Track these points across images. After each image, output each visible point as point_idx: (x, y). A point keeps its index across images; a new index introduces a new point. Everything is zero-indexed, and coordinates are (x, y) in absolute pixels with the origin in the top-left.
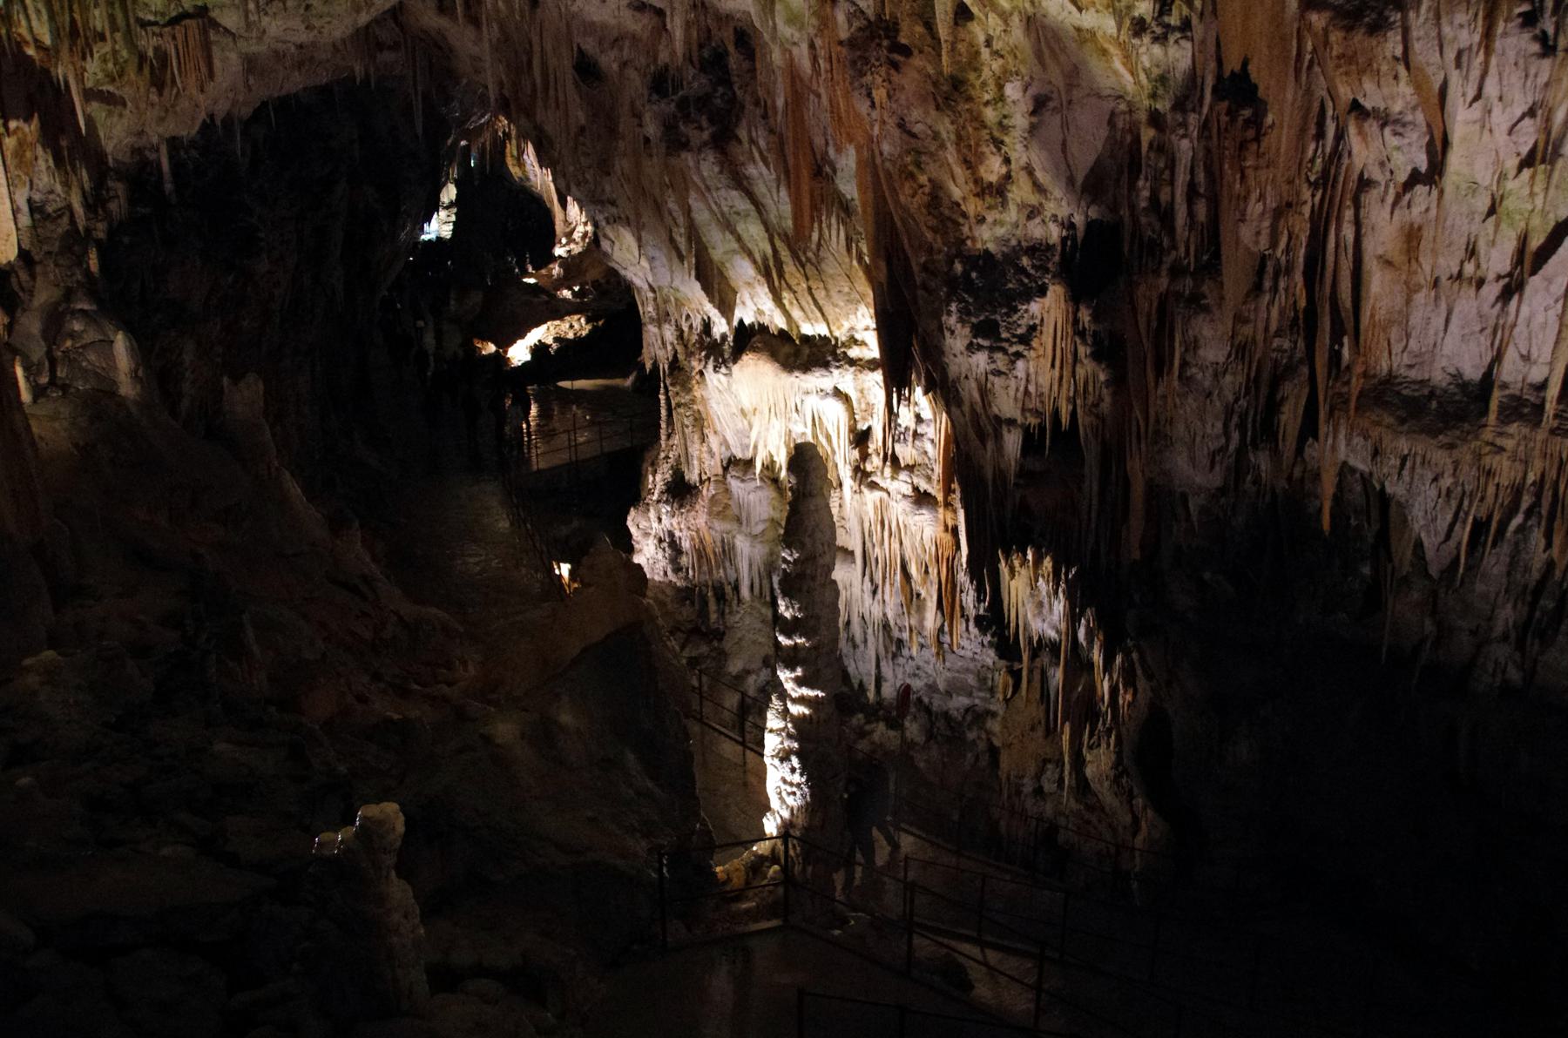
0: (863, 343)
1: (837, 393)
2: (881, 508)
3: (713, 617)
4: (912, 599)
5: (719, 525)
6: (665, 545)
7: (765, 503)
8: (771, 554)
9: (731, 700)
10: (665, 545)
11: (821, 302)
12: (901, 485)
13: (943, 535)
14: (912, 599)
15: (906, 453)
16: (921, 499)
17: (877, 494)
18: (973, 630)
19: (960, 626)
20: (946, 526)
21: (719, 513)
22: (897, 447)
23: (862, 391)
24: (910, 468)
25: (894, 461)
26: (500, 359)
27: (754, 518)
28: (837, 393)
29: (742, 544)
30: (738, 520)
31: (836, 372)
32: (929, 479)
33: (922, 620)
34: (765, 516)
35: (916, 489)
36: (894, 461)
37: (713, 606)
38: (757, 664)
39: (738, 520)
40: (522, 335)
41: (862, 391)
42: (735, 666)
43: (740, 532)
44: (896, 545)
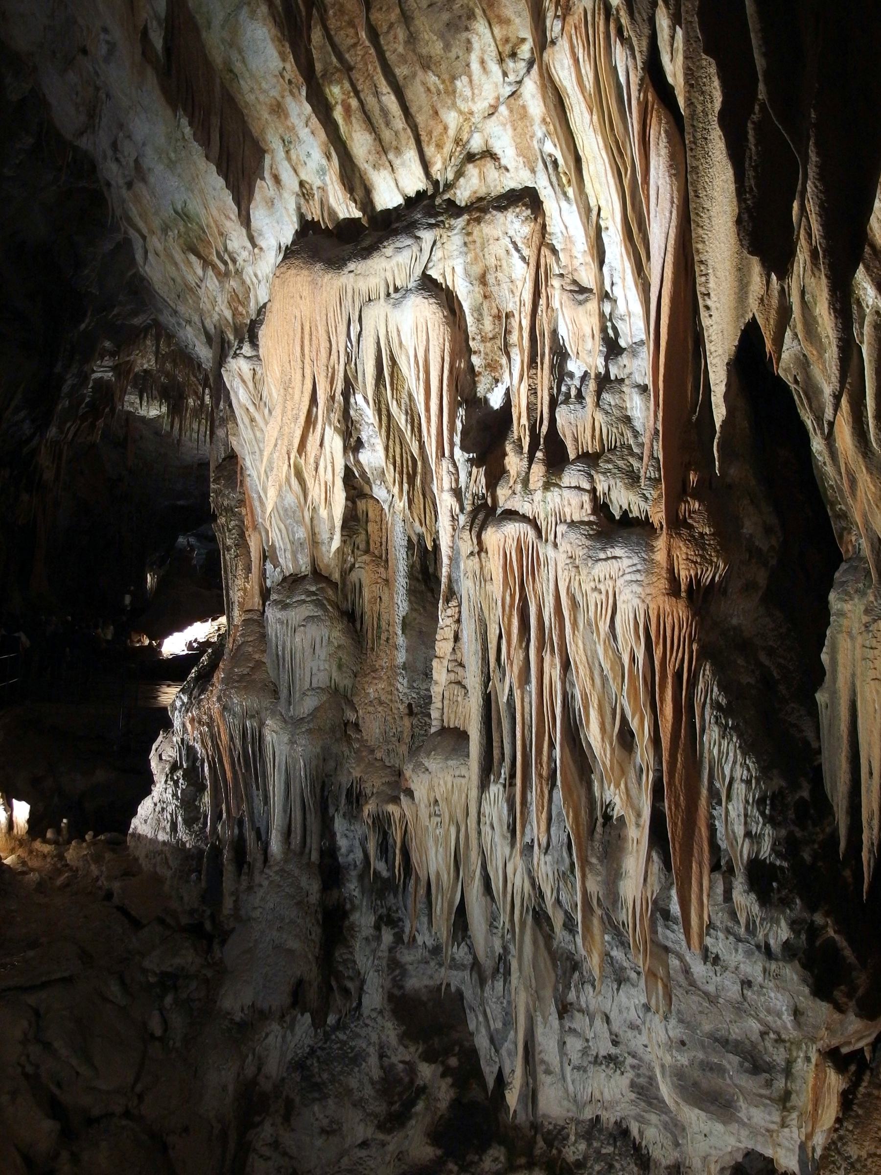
1: (429, 285)
2: (523, 569)
3: (228, 903)
4: (600, 832)
5: (238, 701)
6: (180, 773)
7: (322, 653)
8: (325, 756)
9: (221, 1078)
10: (180, 773)
11: (401, 71)
12: (567, 500)
13: (666, 604)
14: (600, 832)
15: (577, 424)
16: (609, 527)
17: (512, 529)
18: (744, 899)
19: (703, 879)
20: (673, 580)
21: (242, 677)
22: (563, 415)
23: (483, 280)
24: (590, 459)
25: (555, 456)
26: (155, 651)
27: (303, 681)
28: (429, 285)
29: (274, 736)
30: (275, 693)
31: (427, 236)
32: (632, 479)
33: (613, 876)
34: (321, 679)
35: (601, 507)
36: (555, 456)
37: (228, 883)
38: (279, 999)
40: (180, 628)
41: (483, 280)
42: (235, 1000)
43: (273, 713)
44: (553, 670)
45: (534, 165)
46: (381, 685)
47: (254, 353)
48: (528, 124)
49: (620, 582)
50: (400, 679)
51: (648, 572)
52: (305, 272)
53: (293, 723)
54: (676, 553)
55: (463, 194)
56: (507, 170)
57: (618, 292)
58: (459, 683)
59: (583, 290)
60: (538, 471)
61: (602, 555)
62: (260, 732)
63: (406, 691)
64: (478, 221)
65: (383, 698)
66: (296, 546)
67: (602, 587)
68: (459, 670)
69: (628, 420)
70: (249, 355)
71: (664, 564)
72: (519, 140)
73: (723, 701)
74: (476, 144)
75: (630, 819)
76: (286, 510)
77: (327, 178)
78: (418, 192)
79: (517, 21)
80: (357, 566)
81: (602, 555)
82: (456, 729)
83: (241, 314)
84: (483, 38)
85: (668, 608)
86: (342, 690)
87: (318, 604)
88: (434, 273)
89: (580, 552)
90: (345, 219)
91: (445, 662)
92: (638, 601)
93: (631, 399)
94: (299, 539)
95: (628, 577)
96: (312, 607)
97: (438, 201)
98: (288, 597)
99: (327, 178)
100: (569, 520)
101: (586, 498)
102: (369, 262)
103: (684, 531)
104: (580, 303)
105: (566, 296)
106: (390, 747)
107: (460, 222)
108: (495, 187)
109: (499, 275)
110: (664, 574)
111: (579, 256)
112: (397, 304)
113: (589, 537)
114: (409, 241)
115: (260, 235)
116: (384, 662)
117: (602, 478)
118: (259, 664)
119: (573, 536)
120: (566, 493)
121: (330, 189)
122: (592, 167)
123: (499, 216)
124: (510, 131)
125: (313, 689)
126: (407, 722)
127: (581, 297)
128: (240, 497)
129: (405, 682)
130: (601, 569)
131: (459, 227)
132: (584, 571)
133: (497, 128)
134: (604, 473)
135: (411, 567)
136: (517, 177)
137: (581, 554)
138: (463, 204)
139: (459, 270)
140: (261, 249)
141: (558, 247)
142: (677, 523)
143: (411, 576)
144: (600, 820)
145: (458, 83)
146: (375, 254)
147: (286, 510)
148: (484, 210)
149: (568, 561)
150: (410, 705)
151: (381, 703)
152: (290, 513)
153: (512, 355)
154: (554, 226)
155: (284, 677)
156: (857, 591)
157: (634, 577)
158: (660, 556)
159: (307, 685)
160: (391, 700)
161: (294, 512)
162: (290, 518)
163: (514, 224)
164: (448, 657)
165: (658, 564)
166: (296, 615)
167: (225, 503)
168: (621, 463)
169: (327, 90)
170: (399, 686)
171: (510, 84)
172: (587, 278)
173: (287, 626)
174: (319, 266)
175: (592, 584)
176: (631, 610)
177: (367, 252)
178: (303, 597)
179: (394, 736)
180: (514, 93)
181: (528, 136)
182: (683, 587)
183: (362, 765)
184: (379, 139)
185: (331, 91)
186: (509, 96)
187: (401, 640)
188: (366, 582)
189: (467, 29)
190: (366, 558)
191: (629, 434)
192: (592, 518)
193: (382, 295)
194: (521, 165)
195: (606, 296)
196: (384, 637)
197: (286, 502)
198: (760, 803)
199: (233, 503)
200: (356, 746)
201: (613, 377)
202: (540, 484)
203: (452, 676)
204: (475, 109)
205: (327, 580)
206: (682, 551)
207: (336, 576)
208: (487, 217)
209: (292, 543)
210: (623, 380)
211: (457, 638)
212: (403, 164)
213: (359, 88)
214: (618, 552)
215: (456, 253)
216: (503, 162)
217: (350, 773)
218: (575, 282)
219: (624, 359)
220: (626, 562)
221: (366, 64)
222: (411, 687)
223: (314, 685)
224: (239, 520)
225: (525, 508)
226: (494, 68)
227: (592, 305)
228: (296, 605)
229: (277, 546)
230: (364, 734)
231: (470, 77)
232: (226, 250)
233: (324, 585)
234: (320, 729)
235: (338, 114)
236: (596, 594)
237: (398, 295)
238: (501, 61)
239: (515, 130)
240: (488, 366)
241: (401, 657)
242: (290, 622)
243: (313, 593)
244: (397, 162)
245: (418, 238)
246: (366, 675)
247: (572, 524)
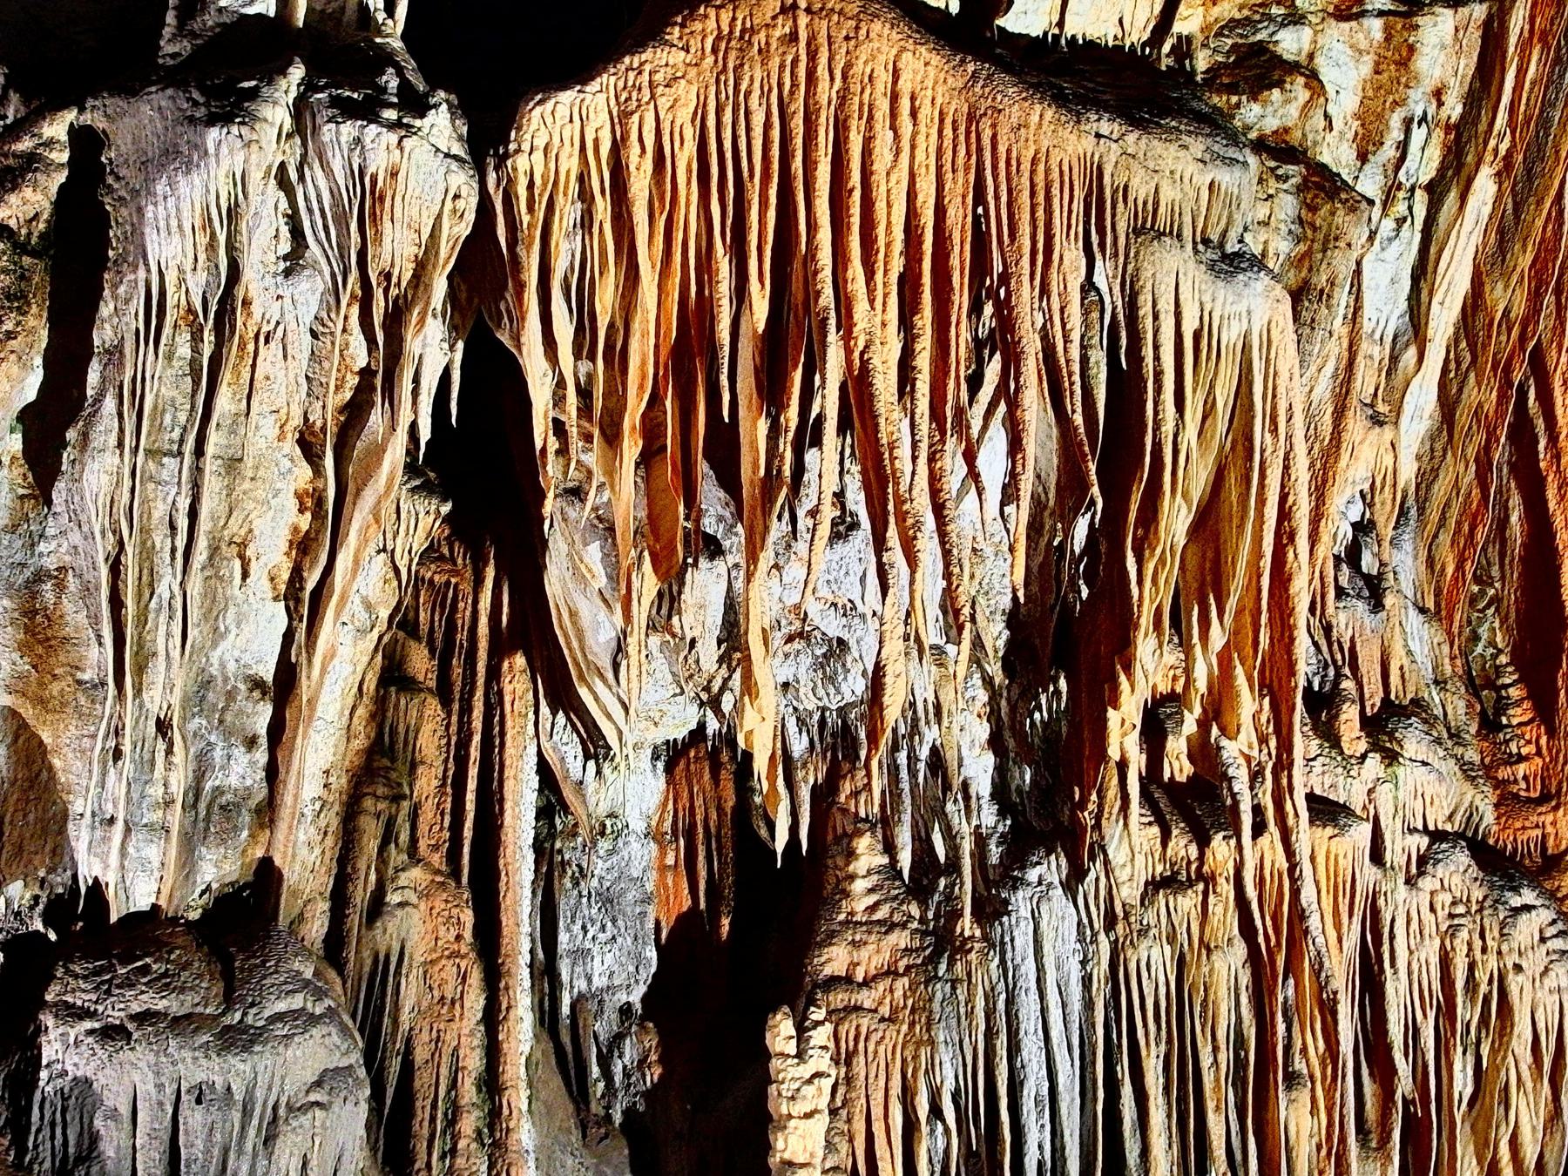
45: (1371, 148)
48: (1403, 80)
72: (1370, 93)
74: (1290, 43)
76: (206, 684)
80: (393, 898)
94: (218, 791)
98: (229, 1001)
100: (1431, 827)
124: (1366, 68)
131: (1293, 181)
133: (1340, 46)
164: (817, 1161)
173: (247, 1113)
178: (297, 1002)
181: (1391, 99)
188: (419, 951)
190: (416, 874)
194: (1350, 135)
196: (469, 1123)
202: (1362, 746)
228: (281, 1030)
229: (77, 806)
239: (1377, 72)
242: (259, 1094)
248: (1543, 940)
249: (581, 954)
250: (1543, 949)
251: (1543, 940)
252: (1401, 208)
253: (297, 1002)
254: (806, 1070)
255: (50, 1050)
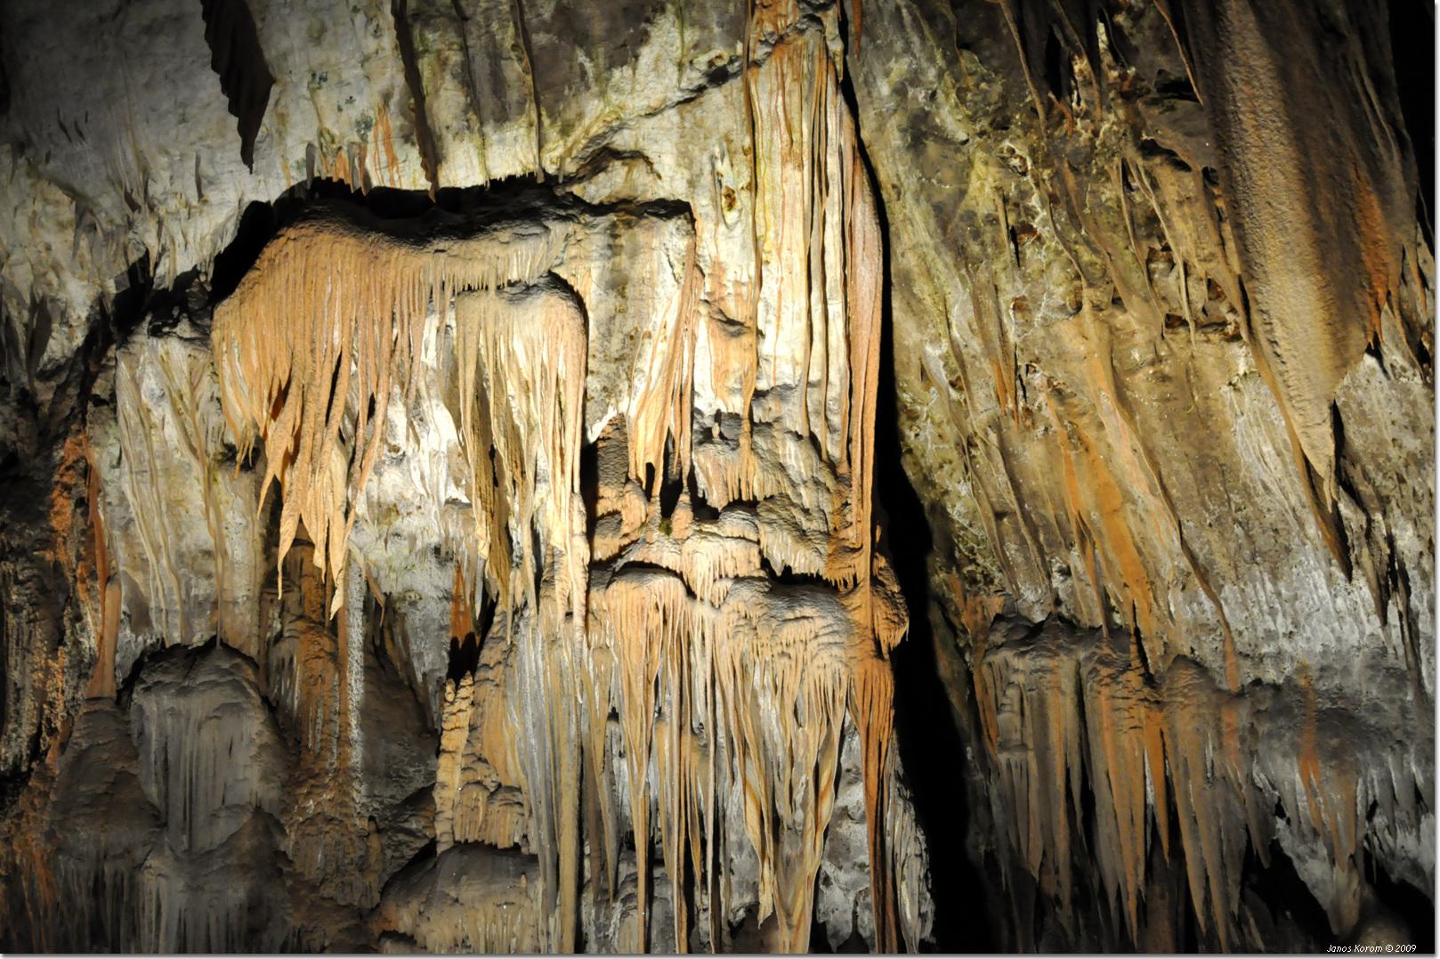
0: (636, 156)
17: (659, 583)
21: (95, 800)
28: (557, 283)
31: (558, 229)
32: (802, 535)
35: (765, 564)
39: (158, 819)
46: (327, 796)
47: (194, 335)
49: (812, 645)
50: (356, 785)
51: (849, 633)
52: (352, 241)
53: (196, 860)
54: (878, 613)
55: (596, 190)
56: (659, 177)
57: (769, 331)
58: (479, 783)
59: (731, 322)
60: (683, 515)
61: (790, 615)
62: (132, 878)
63: (364, 800)
64: (629, 225)
65: (329, 811)
66: (194, 607)
67: (792, 651)
68: (480, 766)
69: (782, 468)
70: (187, 335)
71: (866, 622)
73: (901, 772)
74: (622, 141)
75: (781, 920)
76: (181, 556)
77: (370, 135)
78: (511, 178)
79: (717, 30)
81: (790, 615)
82: (478, 845)
83: (49, 284)
84: (667, 37)
85: (876, 672)
86: (266, 809)
87: (238, 687)
88: (563, 273)
89: (755, 613)
90: (379, 188)
91: (459, 758)
92: (839, 666)
93: (784, 446)
95: (825, 639)
96: (228, 691)
97: (559, 192)
98: (186, 677)
99: (370, 135)
101: (755, 550)
102: (473, 245)
103: (880, 588)
104: (733, 335)
105: (714, 325)
106: (347, 879)
107: (604, 221)
108: (645, 192)
109: (646, 290)
110: (869, 633)
111: (729, 285)
112: (513, 300)
113: (766, 594)
114: (537, 230)
115: (211, 183)
116: (332, 761)
117: (768, 529)
118: (124, 779)
119: (746, 592)
120: (730, 544)
121: (370, 147)
122: (768, 197)
123: (660, 222)
124: (675, 138)
125: (228, 808)
126: (375, 842)
127: (732, 329)
128: (45, 535)
129: (363, 789)
130: (791, 632)
132: (764, 633)
134: (770, 523)
135: (366, 636)
136: (671, 185)
137: (759, 613)
138: (596, 202)
139: (595, 273)
140: (205, 202)
141: (706, 271)
142: (875, 581)
143: (365, 649)
144: (726, 928)
145: (617, 73)
146: (481, 236)
147: (181, 556)
148: (640, 217)
149: (742, 622)
150: (371, 819)
151: (330, 820)
152: (187, 560)
153: (636, 382)
154: (707, 249)
155: (178, 793)
156: (1060, 647)
157: (831, 639)
158: (860, 616)
159: (218, 803)
160: (346, 815)
161: (194, 559)
162: (186, 566)
163: (668, 237)
164: (462, 750)
165: (858, 625)
166: (200, 704)
167: (14, 543)
168: (784, 514)
169: (416, 32)
170: (355, 794)
171: (682, 90)
172: (734, 310)
174: (373, 236)
175: (779, 649)
176: (829, 675)
177: (467, 231)
178: (213, 677)
179: (351, 863)
180: (687, 101)
182: (884, 649)
183: (304, 909)
184: (474, 106)
185: (422, 35)
186: (679, 103)
187: (355, 733)
189: (648, 21)
190: (301, 625)
191: (786, 483)
192: (762, 574)
193: (492, 287)
195: (760, 334)
197: (183, 544)
198: (926, 876)
199: (27, 544)
200: (289, 883)
201: (756, 420)
203: (470, 776)
204: (630, 104)
205: (233, 652)
206: (883, 610)
207: (253, 650)
208: (644, 222)
209: (184, 602)
210: (769, 425)
211: (472, 728)
212: (501, 141)
213: (470, 42)
214: (808, 611)
215: (595, 255)
216: (656, 167)
217: (285, 922)
218: (721, 312)
219: (770, 402)
220: (819, 622)
221: (488, 19)
222: (371, 796)
223: (228, 803)
224: (40, 569)
225: (668, 558)
226: (672, 71)
227: (747, 339)
229: (152, 605)
230: (297, 866)
231: (634, 69)
232: (146, 192)
233: (238, 660)
234: (243, 866)
235: (425, 66)
236: (785, 660)
237: (514, 290)
238: (680, 66)
240: (605, 389)
241: (356, 756)
243: (227, 672)
244: (493, 137)
245: (547, 228)
246: (300, 784)
247: (737, 579)
248: (816, 637)
249: (420, 655)
250: (815, 643)
251: (816, 637)
252: (738, 204)
253: (213, 677)
254: (454, 709)
255: (134, 696)
